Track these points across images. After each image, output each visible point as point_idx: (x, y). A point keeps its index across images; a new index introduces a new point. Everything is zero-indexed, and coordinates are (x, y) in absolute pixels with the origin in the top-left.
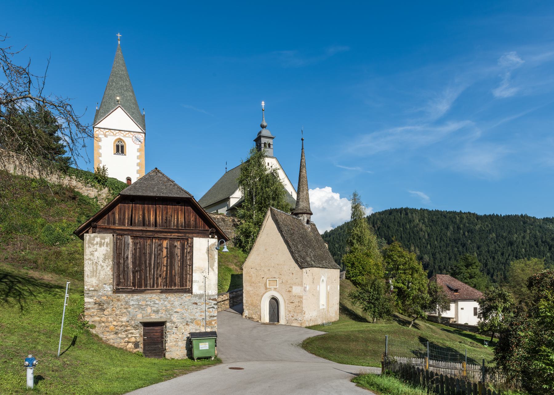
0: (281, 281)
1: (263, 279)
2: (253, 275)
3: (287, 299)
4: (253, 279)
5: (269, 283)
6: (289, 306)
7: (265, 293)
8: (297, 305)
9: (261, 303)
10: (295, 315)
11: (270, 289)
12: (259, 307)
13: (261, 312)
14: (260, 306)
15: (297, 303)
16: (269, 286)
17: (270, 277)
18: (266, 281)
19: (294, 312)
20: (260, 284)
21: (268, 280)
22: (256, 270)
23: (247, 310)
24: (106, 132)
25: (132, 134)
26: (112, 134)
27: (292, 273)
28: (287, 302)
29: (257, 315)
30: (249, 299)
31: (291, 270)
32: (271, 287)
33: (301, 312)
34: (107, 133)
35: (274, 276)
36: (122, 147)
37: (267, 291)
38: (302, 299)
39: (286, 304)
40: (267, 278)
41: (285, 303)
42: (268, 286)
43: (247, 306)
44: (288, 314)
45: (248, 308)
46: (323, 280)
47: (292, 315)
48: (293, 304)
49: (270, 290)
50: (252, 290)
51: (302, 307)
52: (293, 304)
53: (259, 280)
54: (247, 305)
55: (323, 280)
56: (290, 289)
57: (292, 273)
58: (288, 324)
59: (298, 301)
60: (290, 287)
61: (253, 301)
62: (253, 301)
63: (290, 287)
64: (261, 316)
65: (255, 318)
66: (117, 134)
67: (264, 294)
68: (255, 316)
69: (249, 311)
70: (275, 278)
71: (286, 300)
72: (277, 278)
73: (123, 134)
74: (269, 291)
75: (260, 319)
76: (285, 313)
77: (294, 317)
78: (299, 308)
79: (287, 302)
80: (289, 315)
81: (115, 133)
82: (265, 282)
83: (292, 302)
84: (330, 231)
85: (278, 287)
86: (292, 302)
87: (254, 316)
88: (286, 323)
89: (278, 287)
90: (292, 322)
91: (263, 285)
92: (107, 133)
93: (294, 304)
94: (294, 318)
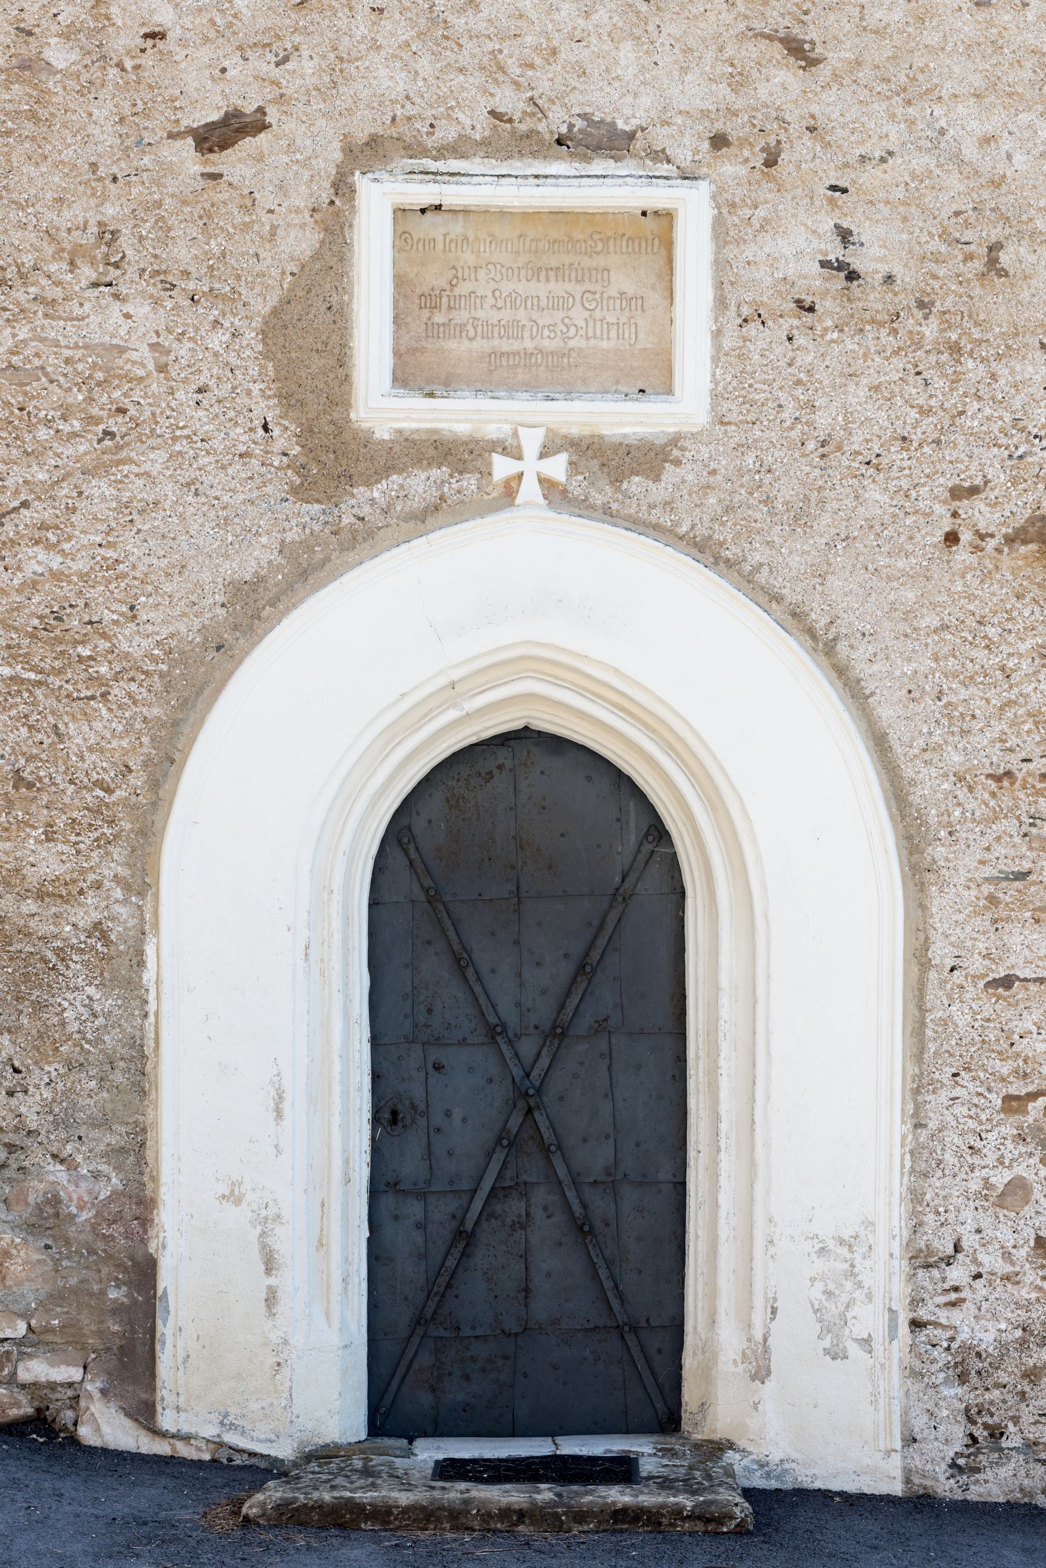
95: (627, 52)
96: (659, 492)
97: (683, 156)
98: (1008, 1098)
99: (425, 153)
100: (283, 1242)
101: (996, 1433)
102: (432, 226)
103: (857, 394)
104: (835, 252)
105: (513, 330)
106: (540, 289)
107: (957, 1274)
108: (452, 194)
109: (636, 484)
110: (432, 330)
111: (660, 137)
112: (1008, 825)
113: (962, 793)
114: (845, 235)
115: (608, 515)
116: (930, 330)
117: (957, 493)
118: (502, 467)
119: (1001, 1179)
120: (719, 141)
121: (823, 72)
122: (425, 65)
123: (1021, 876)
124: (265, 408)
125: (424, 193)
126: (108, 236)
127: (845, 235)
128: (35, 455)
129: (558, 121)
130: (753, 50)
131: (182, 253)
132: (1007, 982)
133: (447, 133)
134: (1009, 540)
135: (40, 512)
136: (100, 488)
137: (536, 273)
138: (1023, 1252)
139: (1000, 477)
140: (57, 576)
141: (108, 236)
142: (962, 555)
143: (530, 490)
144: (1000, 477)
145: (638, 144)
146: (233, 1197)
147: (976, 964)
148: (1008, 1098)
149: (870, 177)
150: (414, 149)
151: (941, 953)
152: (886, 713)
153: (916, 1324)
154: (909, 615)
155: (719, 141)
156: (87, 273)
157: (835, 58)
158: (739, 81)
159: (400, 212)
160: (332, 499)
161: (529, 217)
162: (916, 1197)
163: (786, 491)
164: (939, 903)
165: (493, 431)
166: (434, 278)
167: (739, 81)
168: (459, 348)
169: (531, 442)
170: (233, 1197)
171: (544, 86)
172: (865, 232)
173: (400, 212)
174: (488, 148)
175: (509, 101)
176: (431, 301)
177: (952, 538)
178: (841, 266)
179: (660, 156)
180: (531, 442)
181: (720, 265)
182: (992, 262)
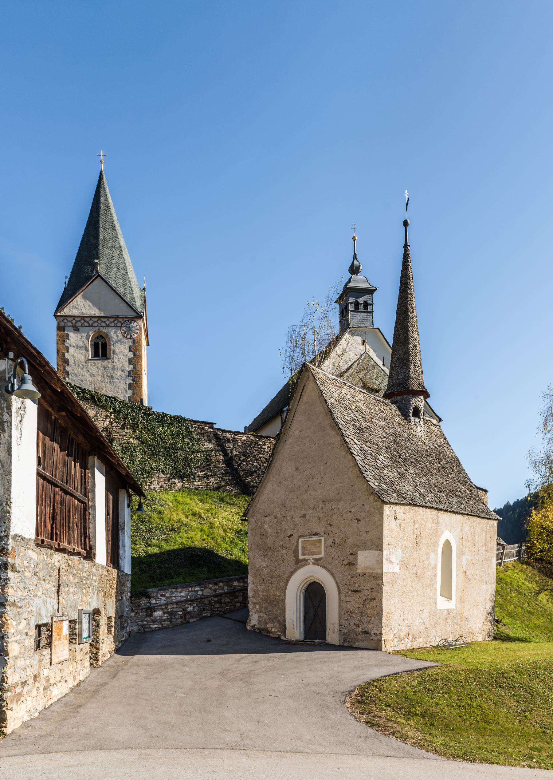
0: (330, 541)
1: (291, 538)
2: (269, 530)
4: (270, 541)
5: (304, 548)
6: (348, 599)
7: (296, 570)
8: (369, 597)
9: (285, 595)
10: (365, 620)
11: (306, 560)
12: (281, 604)
13: (284, 616)
14: (283, 601)
15: (368, 592)
16: (303, 554)
17: (307, 533)
18: (298, 543)
19: (361, 613)
20: (284, 551)
21: (300, 540)
22: (276, 520)
23: (257, 612)
24: (77, 322)
25: (120, 322)
26: (86, 324)
27: (358, 520)
28: (343, 592)
29: (277, 625)
30: (260, 588)
31: (353, 510)
32: (306, 557)
34: (79, 324)
40: (300, 537)
43: (257, 604)
45: (258, 607)
47: (357, 622)
48: (359, 594)
50: (267, 567)
52: (357, 595)
54: (255, 600)
56: (351, 559)
58: (346, 644)
60: (352, 554)
61: (268, 590)
62: (268, 590)
63: (352, 554)
64: (285, 626)
65: (273, 630)
66: (96, 324)
67: (292, 573)
68: (272, 625)
69: (261, 614)
70: (316, 534)
71: (340, 585)
72: (322, 534)
73: (105, 322)
74: (304, 565)
75: (284, 633)
76: (340, 617)
77: (362, 627)
78: (373, 603)
81: (91, 322)
82: (295, 544)
83: (356, 591)
84: (515, 503)
86: (356, 591)
87: (270, 626)
88: (342, 641)
90: (357, 640)
91: (291, 553)
92: (79, 324)
93: (361, 594)
94: (360, 630)
95: (318, 527)
96: (320, 562)
97: (322, 535)
100: (294, 624)
101: (346, 640)
102: (304, 542)
103: (335, 553)
105: (310, 550)
106: (312, 546)
107: (343, 626)
108: (305, 540)
109: (319, 562)
110: (305, 550)
111: (321, 533)
112: (346, 589)
114: (334, 540)
115: (317, 565)
116: (340, 547)
117: (343, 561)
118: (309, 561)
119: (346, 618)
120: (325, 533)
122: (304, 529)
124: (293, 557)
125: (303, 540)
126: (282, 545)
127: (334, 540)
128: (278, 562)
129: (313, 533)
130: (327, 525)
131: (287, 546)
136: (282, 565)
137: (312, 545)
141: (282, 545)
142: (343, 566)
143: (311, 563)
146: (291, 620)
149: (336, 535)
150: (303, 536)
151: (342, 599)
152: (337, 579)
153: (340, 631)
154: (339, 571)
155: (325, 533)
157: (333, 525)
158: (326, 528)
159: (302, 541)
160: (297, 564)
161: (311, 540)
162: (340, 620)
163: (330, 561)
164: (341, 595)
165: (308, 558)
166: (305, 546)
167: (326, 528)
168: (307, 552)
169: (311, 559)
170: (291, 620)
172: (335, 540)
173: (302, 541)
174: (309, 535)
175: (310, 531)
176: (305, 548)
179: (321, 535)
180: (311, 559)
181: (325, 543)
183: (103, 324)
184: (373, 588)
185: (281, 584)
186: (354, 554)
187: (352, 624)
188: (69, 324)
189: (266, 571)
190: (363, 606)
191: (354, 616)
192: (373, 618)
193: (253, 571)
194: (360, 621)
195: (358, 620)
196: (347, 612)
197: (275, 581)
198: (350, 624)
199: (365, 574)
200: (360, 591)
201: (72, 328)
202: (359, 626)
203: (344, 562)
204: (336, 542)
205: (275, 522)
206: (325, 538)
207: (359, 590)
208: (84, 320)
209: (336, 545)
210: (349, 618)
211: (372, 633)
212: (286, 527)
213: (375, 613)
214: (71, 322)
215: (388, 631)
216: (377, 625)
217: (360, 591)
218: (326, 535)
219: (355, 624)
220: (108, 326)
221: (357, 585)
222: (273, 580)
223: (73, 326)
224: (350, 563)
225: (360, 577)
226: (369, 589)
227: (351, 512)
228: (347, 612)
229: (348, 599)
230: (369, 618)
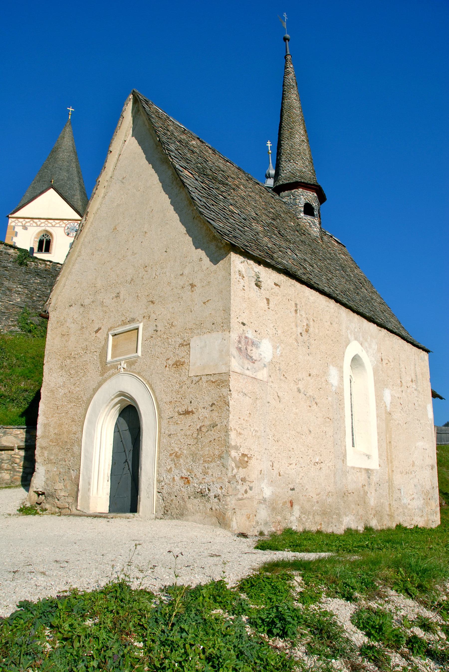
0: (151, 329)
3: (168, 399)
6: (173, 429)
8: (207, 423)
10: (198, 471)
15: (206, 413)
16: (113, 357)
18: (107, 339)
24: (27, 222)
25: (65, 223)
26: (34, 225)
27: (192, 286)
31: (186, 272)
33: (220, 457)
34: (28, 224)
35: (132, 316)
36: (49, 243)
37: (105, 380)
38: (224, 391)
39: (164, 422)
40: (110, 330)
41: (160, 417)
42: (109, 358)
44: (170, 471)
46: (356, 360)
47: (185, 473)
48: (190, 417)
49: (113, 374)
51: (227, 431)
52: (188, 420)
53: (86, 340)
55: (356, 360)
57: (192, 286)
59: (208, 400)
60: (182, 345)
63: (182, 345)
66: (43, 225)
73: (51, 223)
77: (195, 483)
78: (213, 434)
79: (168, 412)
80: (175, 471)
81: (39, 223)
83: (187, 413)
85: (139, 353)
86: (187, 413)
89: (139, 353)
91: (96, 357)
92: (28, 224)
97: (140, 320)
98: (170, 454)
99: (115, 327)
104: (155, 328)
113: (166, 405)
114: (156, 326)
121: (155, 304)
123: (172, 417)
124: (99, 365)
127: (156, 326)
132: (170, 435)
133: (117, 324)
134: (173, 365)
135: (78, 383)
136: (84, 379)
138: (171, 480)
139: (172, 356)
140: (79, 391)
142: (167, 369)
144: (172, 356)
145: (136, 320)
147: (167, 432)
148: (170, 454)
151: (163, 431)
152: (157, 394)
155: (144, 317)
156: (85, 352)
171: (127, 315)
172: (158, 325)
175: (124, 318)
177: (166, 366)
178: (156, 330)
182: (172, 325)
183: (50, 225)
184: (213, 404)
185: (78, 411)
186: (186, 344)
187: (177, 478)
188: (20, 224)
189: (62, 391)
190: (196, 441)
191: (181, 461)
192: (212, 465)
193: (46, 394)
194: (191, 471)
195: (188, 470)
196: (171, 455)
197: (71, 408)
198: (174, 478)
199: (201, 379)
200: (192, 412)
201: (21, 227)
202: (188, 482)
203: (170, 362)
204: (159, 329)
205: (81, 312)
206: (144, 325)
207: (190, 410)
208: (33, 221)
209: (159, 333)
210: (173, 466)
211: (212, 494)
212: (94, 318)
213: (217, 453)
214: (21, 222)
215: (242, 491)
216: (220, 478)
217: (192, 412)
218: (145, 320)
219: (182, 478)
220: (53, 226)
221: (187, 401)
222: (69, 406)
223: (22, 226)
224: (179, 361)
225: (193, 385)
226: (207, 406)
227: (182, 275)
228: (171, 455)
229: (173, 429)
230: (206, 465)
